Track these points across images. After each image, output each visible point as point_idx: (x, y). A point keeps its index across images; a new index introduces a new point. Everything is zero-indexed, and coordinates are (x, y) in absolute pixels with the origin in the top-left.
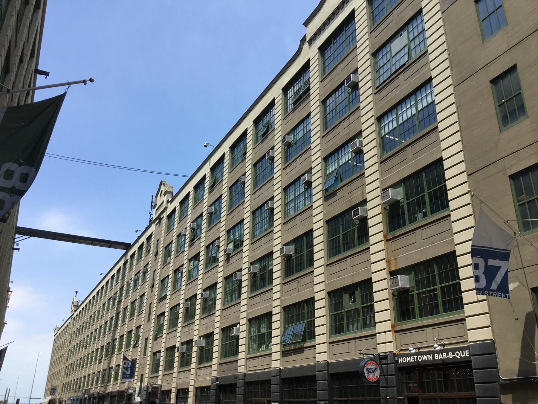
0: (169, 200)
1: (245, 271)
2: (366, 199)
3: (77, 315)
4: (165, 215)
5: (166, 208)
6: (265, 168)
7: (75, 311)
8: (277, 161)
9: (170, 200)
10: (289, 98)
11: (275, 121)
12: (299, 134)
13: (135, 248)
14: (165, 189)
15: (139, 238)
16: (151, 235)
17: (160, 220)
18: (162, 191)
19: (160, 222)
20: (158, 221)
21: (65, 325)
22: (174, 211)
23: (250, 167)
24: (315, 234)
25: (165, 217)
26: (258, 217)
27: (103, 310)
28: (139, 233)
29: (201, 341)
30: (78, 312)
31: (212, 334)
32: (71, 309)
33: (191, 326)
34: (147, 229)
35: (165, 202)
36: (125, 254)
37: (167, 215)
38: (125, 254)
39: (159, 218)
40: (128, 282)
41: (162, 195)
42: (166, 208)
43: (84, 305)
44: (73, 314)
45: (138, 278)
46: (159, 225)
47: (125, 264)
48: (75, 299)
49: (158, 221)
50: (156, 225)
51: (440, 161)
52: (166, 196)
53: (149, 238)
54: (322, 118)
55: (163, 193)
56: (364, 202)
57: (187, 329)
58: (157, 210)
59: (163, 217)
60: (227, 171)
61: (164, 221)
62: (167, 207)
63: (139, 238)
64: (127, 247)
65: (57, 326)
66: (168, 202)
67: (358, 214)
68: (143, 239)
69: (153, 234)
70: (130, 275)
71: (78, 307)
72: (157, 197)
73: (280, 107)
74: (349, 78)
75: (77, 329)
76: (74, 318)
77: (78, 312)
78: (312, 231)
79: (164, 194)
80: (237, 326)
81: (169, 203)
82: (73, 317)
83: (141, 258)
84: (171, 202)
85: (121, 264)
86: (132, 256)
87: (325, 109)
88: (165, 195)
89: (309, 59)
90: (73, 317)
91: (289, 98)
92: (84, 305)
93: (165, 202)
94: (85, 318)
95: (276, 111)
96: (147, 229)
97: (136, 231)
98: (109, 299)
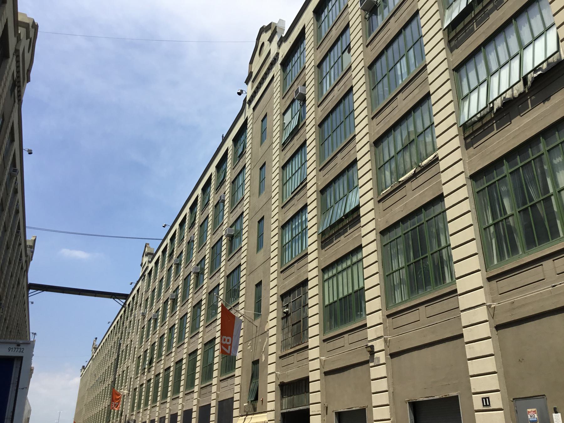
3: (96, 356)
5: (147, 267)
9: (150, 260)
13: (130, 299)
15: (133, 289)
17: (145, 276)
19: (144, 278)
34: (138, 282)
36: (125, 304)
38: (125, 304)
43: (100, 347)
44: (93, 356)
47: (125, 311)
50: (142, 280)
53: (138, 291)
58: (143, 268)
59: (146, 274)
62: (148, 267)
63: (133, 289)
64: (126, 297)
68: (135, 291)
69: (140, 287)
76: (94, 359)
86: (129, 305)
90: (93, 358)
92: (100, 347)
93: (147, 263)
96: (138, 282)
97: (130, 283)
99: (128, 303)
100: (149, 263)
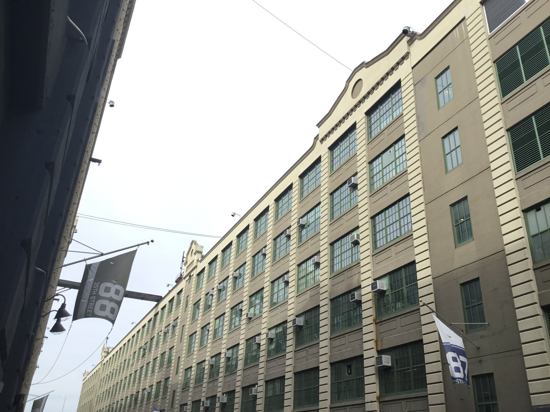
0: (198, 259)
1: (263, 336)
2: (361, 286)
4: (195, 272)
5: (196, 267)
6: (283, 244)
7: (105, 357)
8: (292, 240)
9: (200, 260)
10: (304, 185)
11: (292, 204)
12: (311, 217)
13: (165, 302)
14: (196, 249)
15: (170, 291)
16: (181, 291)
18: (193, 250)
19: (190, 279)
20: (188, 278)
21: (95, 371)
22: (203, 270)
23: (270, 241)
24: (322, 310)
25: (195, 276)
26: (276, 287)
27: (134, 358)
28: (170, 288)
29: (224, 398)
30: (108, 358)
31: (234, 392)
32: (101, 355)
33: (215, 383)
35: (195, 261)
36: (157, 305)
37: (197, 274)
38: (157, 305)
39: (190, 275)
40: (158, 334)
41: (193, 254)
42: (196, 267)
43: (114, 352)
44: (103, 360)
45: (168, 331)
46: (189, 282)
47: (156, 315)
48: (105, 345)
49: (188, 278)
50: (186, 281)
51: (413, 263)
52: (196, 255)
53: (179, 293)
54: (329, 208)
55: (194, 252)
56: (359, 287)
57: (211, 385)
58: (187, 267)
60: (251, 241)
61: (194, 278)
64: (158, 299)
65: (87, 371)
66: (198, 261)
67: (354, 298)
68: (174, 293)
69: (183, 290)
70: (160, 327)
71: (108, 353)
72: (188, 255)
73: (297, 192)
74: (350, 179)
75: (107, 375)
76: (104, 364)
77: (108, 358)
78: (318, 307)
79: (194, 254)
80: (255, 387)
81: (199, 262)
82: (103, 362)
83: (171, 311)
84: (201, 261)
85: (152, 315)
87: (332, 201)
88: (195, 254)
89: (321, 156)
91: (304, 185)
93: (195, 261)
94: (115, 365)
95: (293, 195)
98: (140, 349)
99: (161, 305)
100: (198, 262)
